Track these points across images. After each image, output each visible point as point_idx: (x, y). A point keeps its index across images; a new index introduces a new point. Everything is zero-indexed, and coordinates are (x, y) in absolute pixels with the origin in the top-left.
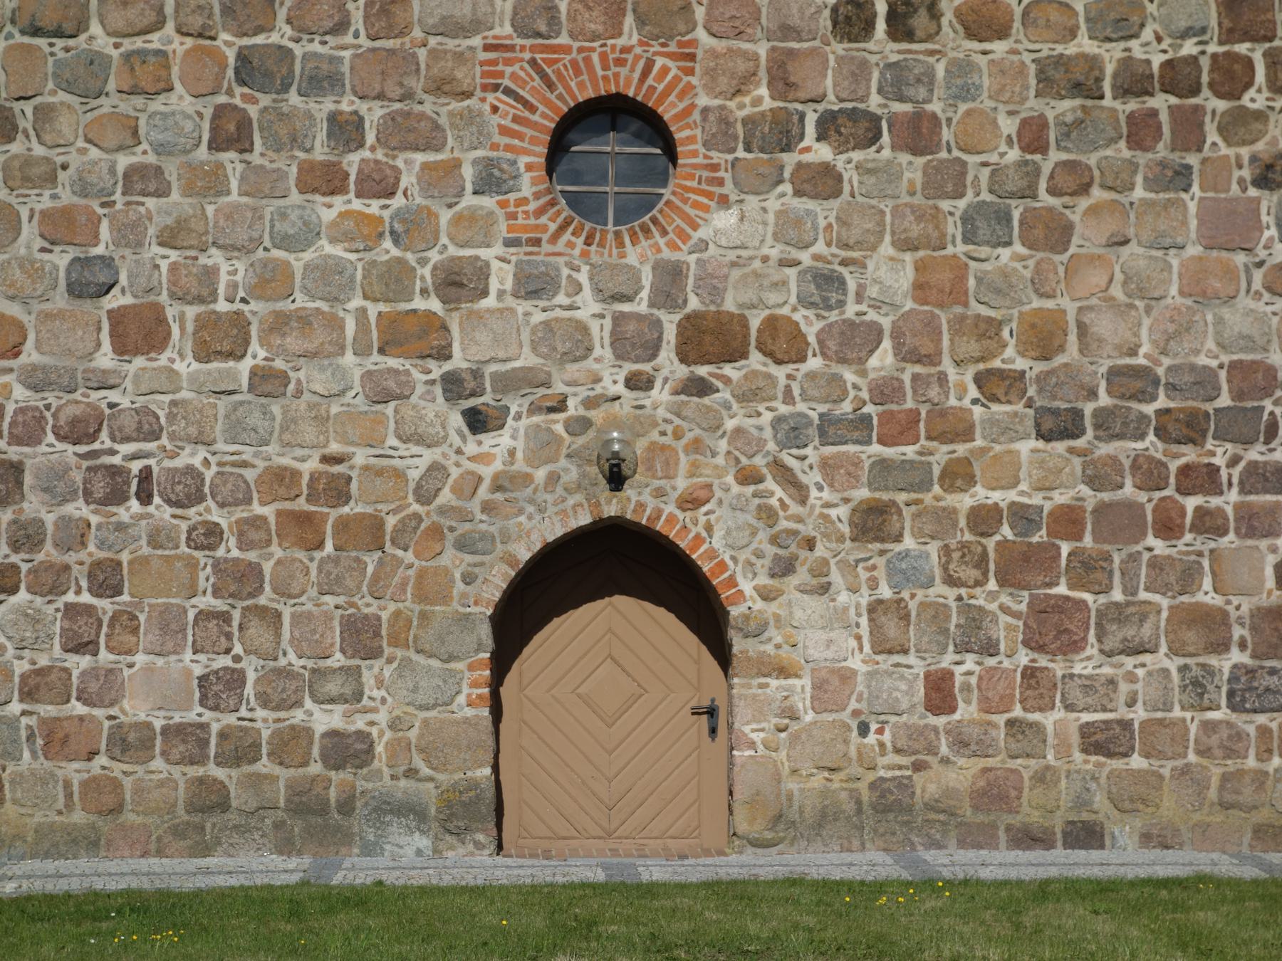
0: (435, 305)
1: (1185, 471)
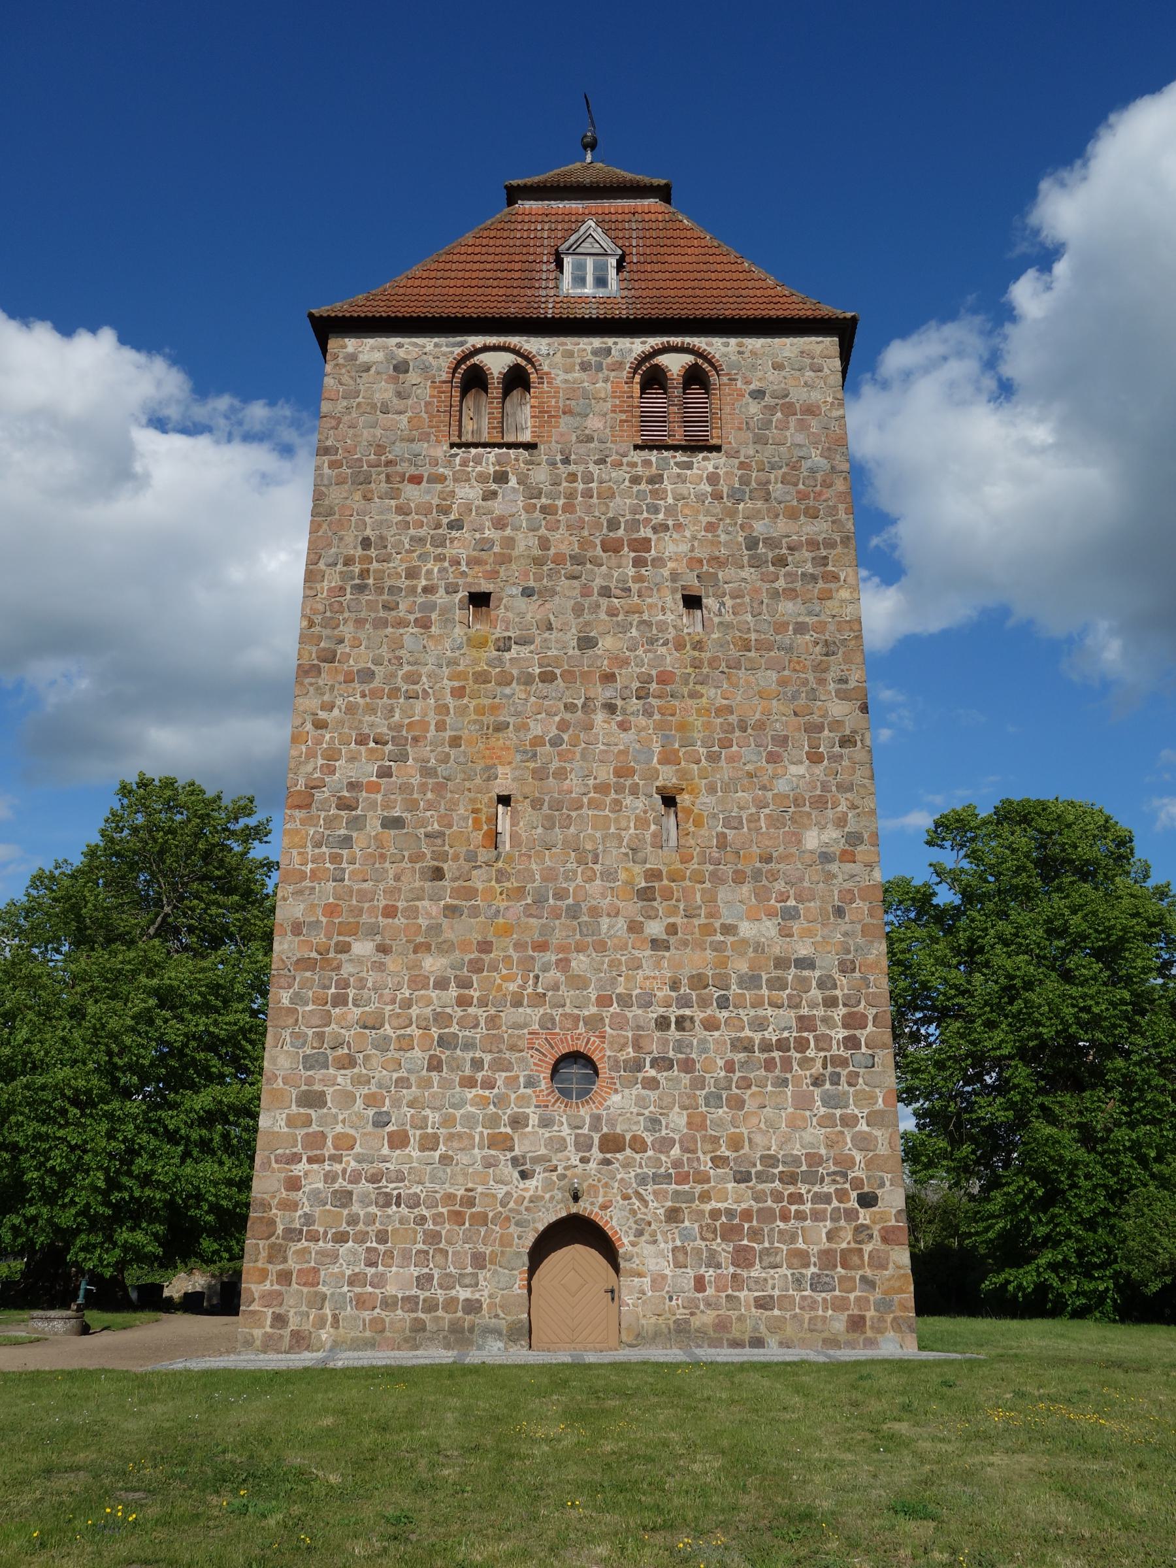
0: (509, 1130)
1: (790, 1195)
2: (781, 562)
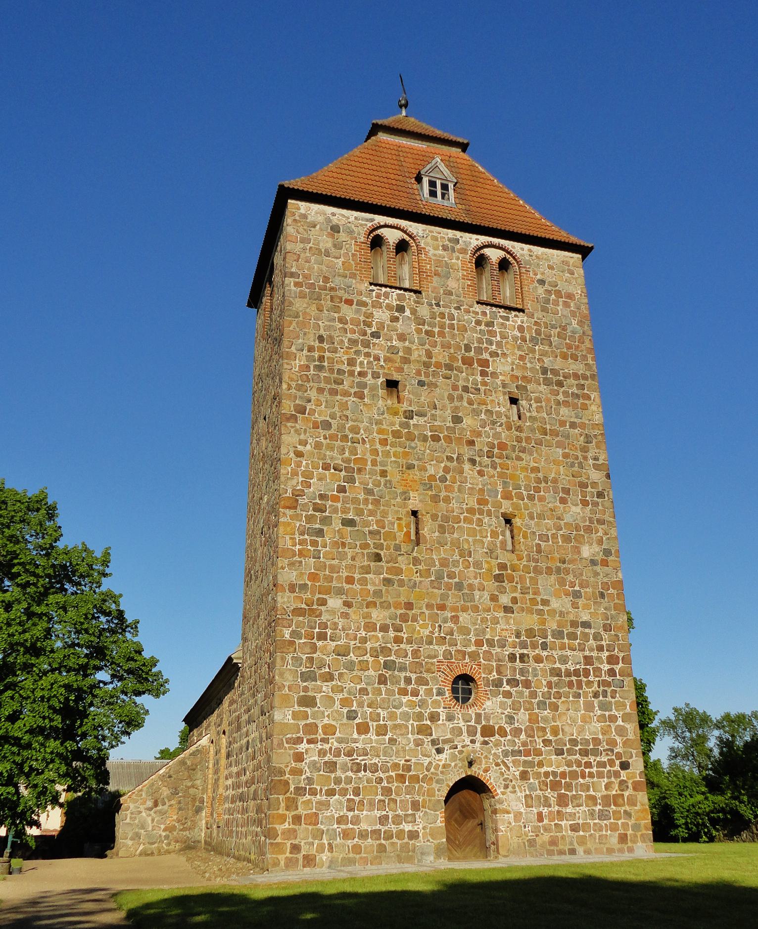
0: (429, 723)
1: (586, 763)
2: (560, 384)
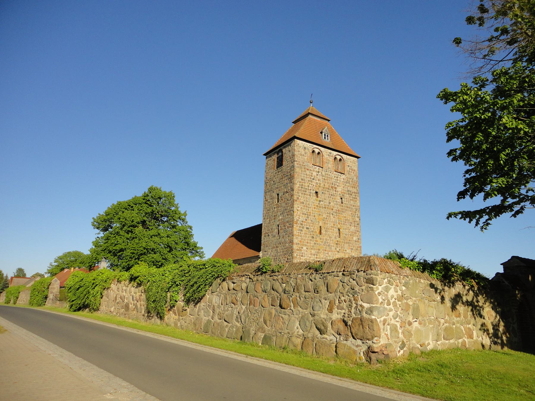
2: (351, 195)
